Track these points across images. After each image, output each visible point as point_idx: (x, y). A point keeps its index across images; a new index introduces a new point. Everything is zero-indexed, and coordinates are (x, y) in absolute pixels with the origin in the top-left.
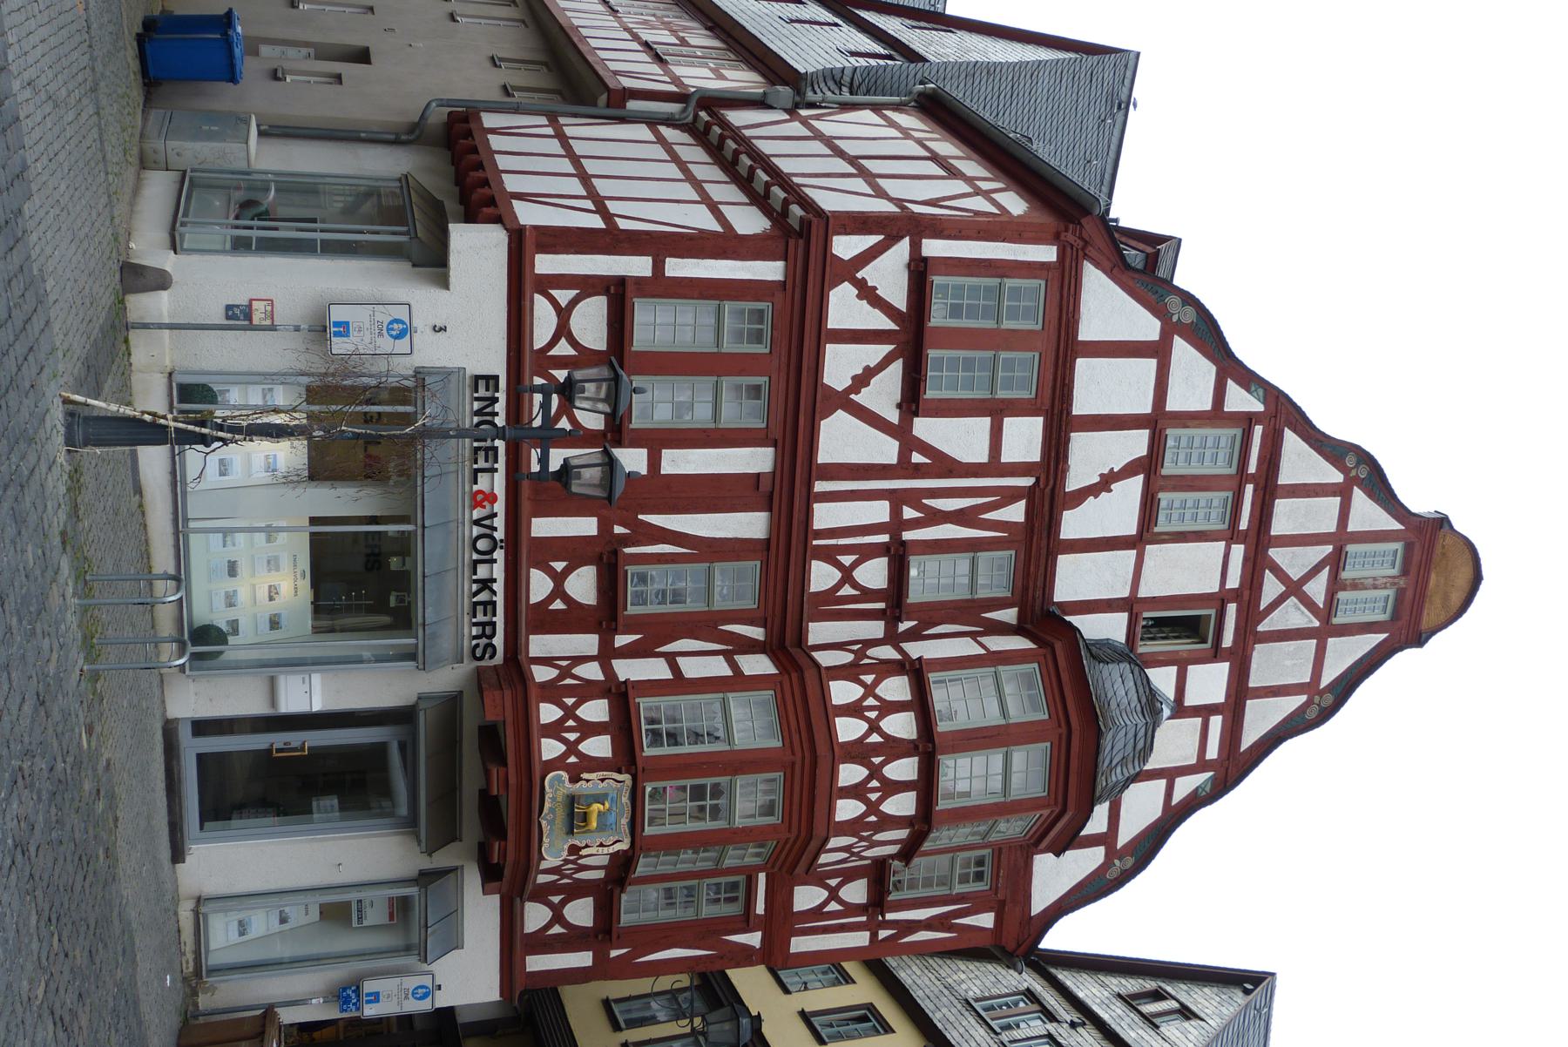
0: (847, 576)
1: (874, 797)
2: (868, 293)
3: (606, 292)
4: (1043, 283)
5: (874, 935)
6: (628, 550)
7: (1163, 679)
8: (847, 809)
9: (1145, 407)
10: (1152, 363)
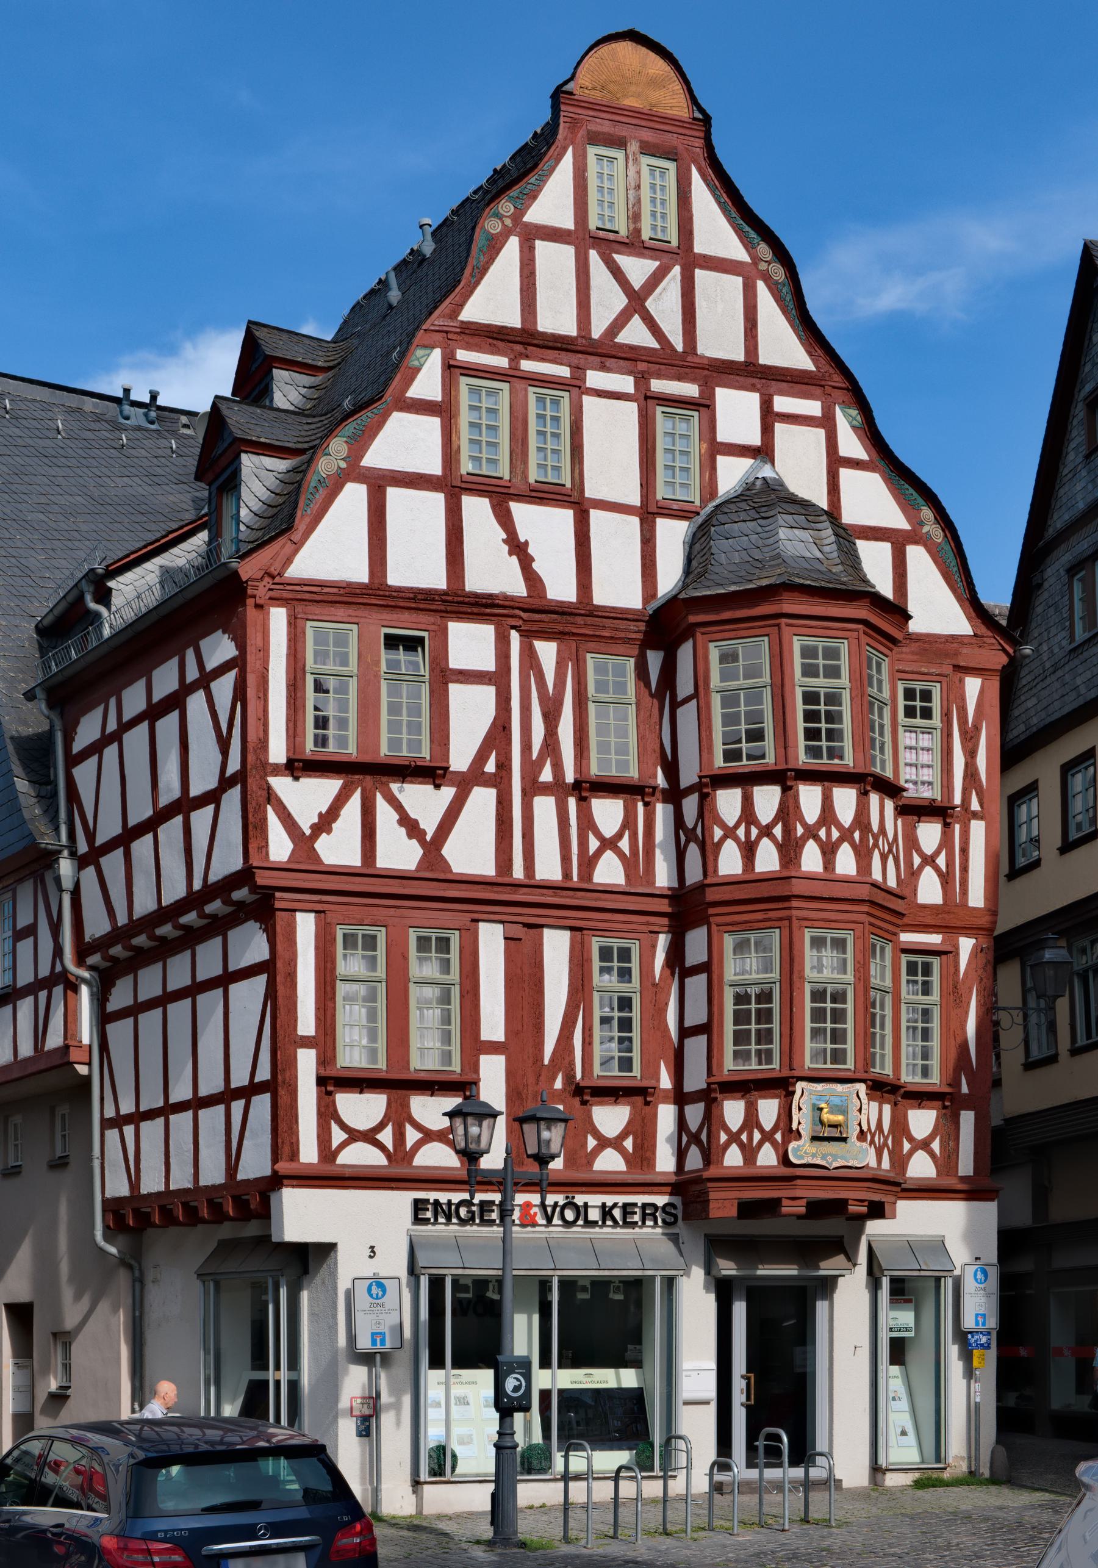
1: (835, 834)
2: (326, 822)
3: (329, 1093)
4: (309, 624)
5: (975, 815)
6: (579, 1076)
7: (732, 474)
8: (846, 863)
9: (437, 501)
10: (393, 494)
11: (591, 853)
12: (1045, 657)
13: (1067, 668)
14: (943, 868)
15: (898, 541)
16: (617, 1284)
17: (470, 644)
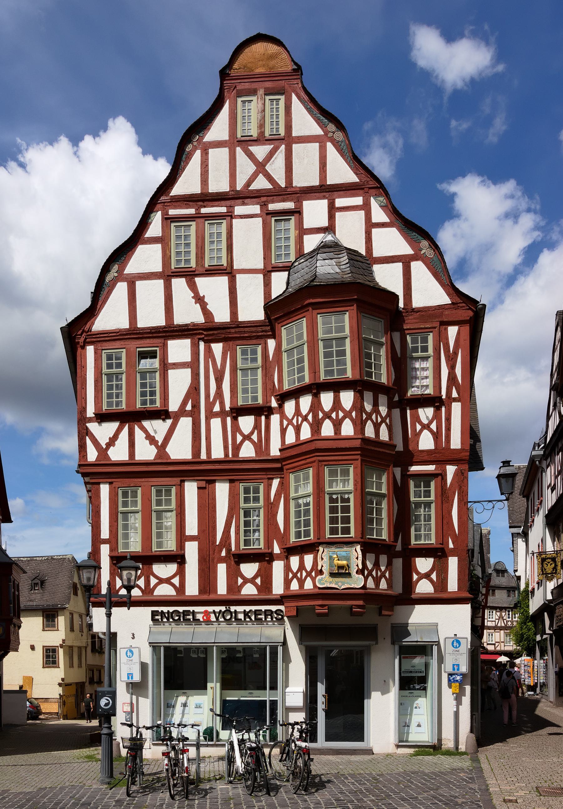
0: (247, 437)
4: (104, 351)
5: (455, 400)
11: (238, 443)
14: (435, 430)
15: (406, 261)
16: (202, 649)
17: (179, 350)
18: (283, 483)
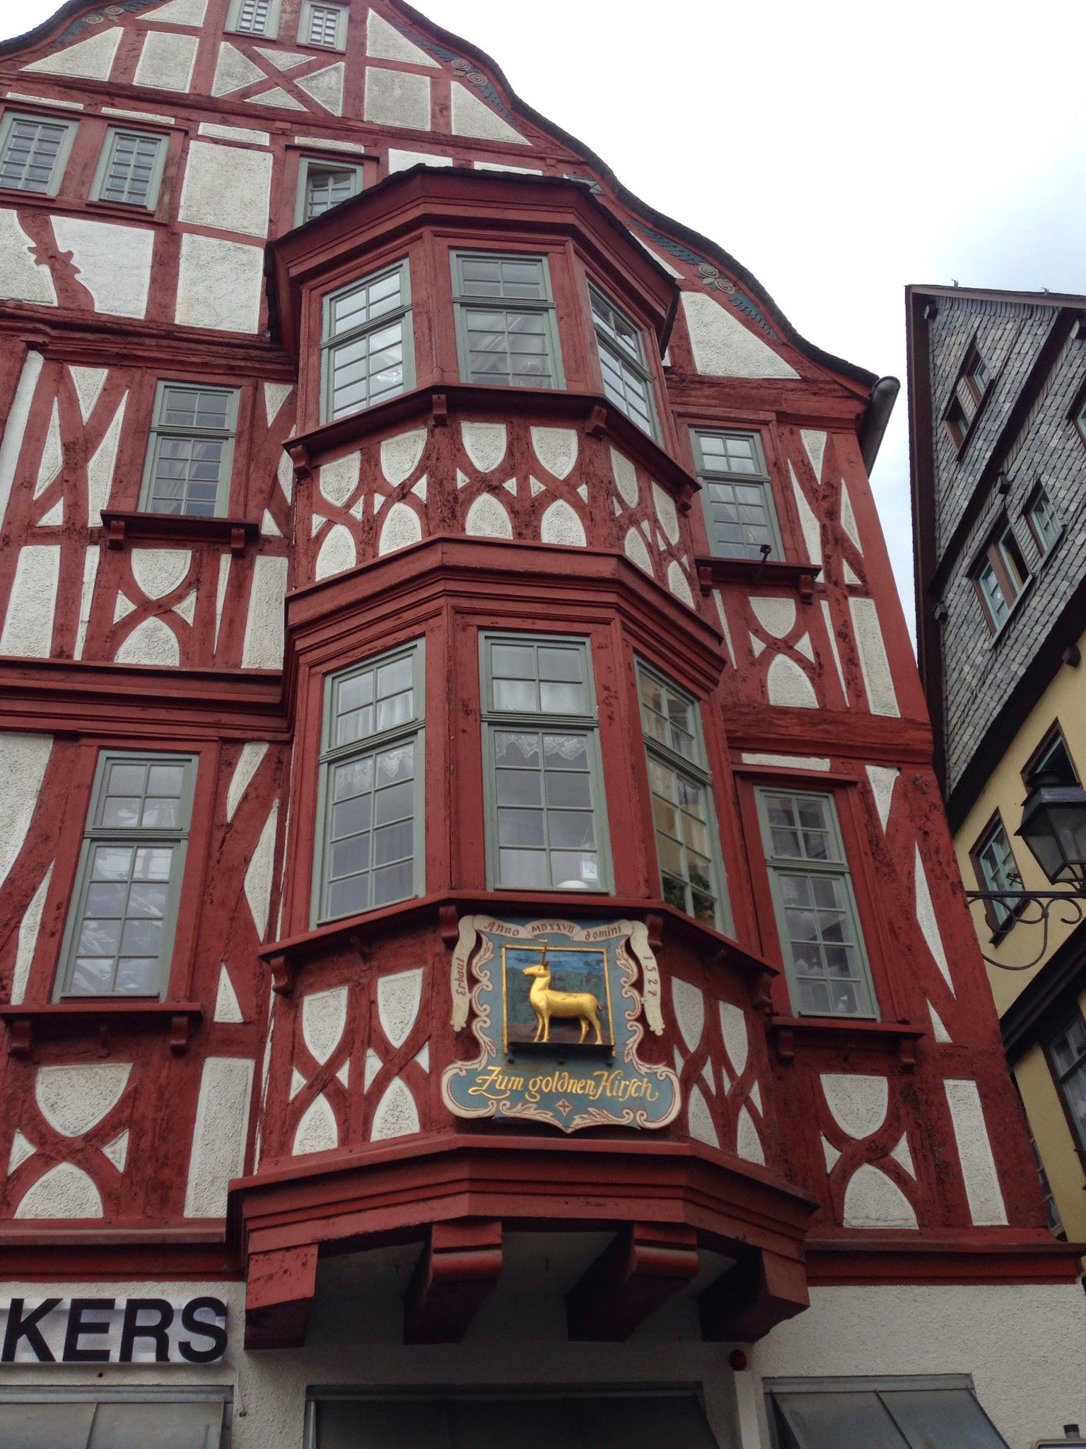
12: (969, 678)
13: (997, 666)
14: (811, 656)
18: (280, 762)
